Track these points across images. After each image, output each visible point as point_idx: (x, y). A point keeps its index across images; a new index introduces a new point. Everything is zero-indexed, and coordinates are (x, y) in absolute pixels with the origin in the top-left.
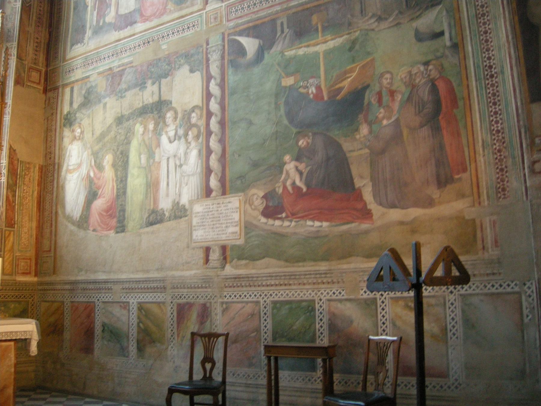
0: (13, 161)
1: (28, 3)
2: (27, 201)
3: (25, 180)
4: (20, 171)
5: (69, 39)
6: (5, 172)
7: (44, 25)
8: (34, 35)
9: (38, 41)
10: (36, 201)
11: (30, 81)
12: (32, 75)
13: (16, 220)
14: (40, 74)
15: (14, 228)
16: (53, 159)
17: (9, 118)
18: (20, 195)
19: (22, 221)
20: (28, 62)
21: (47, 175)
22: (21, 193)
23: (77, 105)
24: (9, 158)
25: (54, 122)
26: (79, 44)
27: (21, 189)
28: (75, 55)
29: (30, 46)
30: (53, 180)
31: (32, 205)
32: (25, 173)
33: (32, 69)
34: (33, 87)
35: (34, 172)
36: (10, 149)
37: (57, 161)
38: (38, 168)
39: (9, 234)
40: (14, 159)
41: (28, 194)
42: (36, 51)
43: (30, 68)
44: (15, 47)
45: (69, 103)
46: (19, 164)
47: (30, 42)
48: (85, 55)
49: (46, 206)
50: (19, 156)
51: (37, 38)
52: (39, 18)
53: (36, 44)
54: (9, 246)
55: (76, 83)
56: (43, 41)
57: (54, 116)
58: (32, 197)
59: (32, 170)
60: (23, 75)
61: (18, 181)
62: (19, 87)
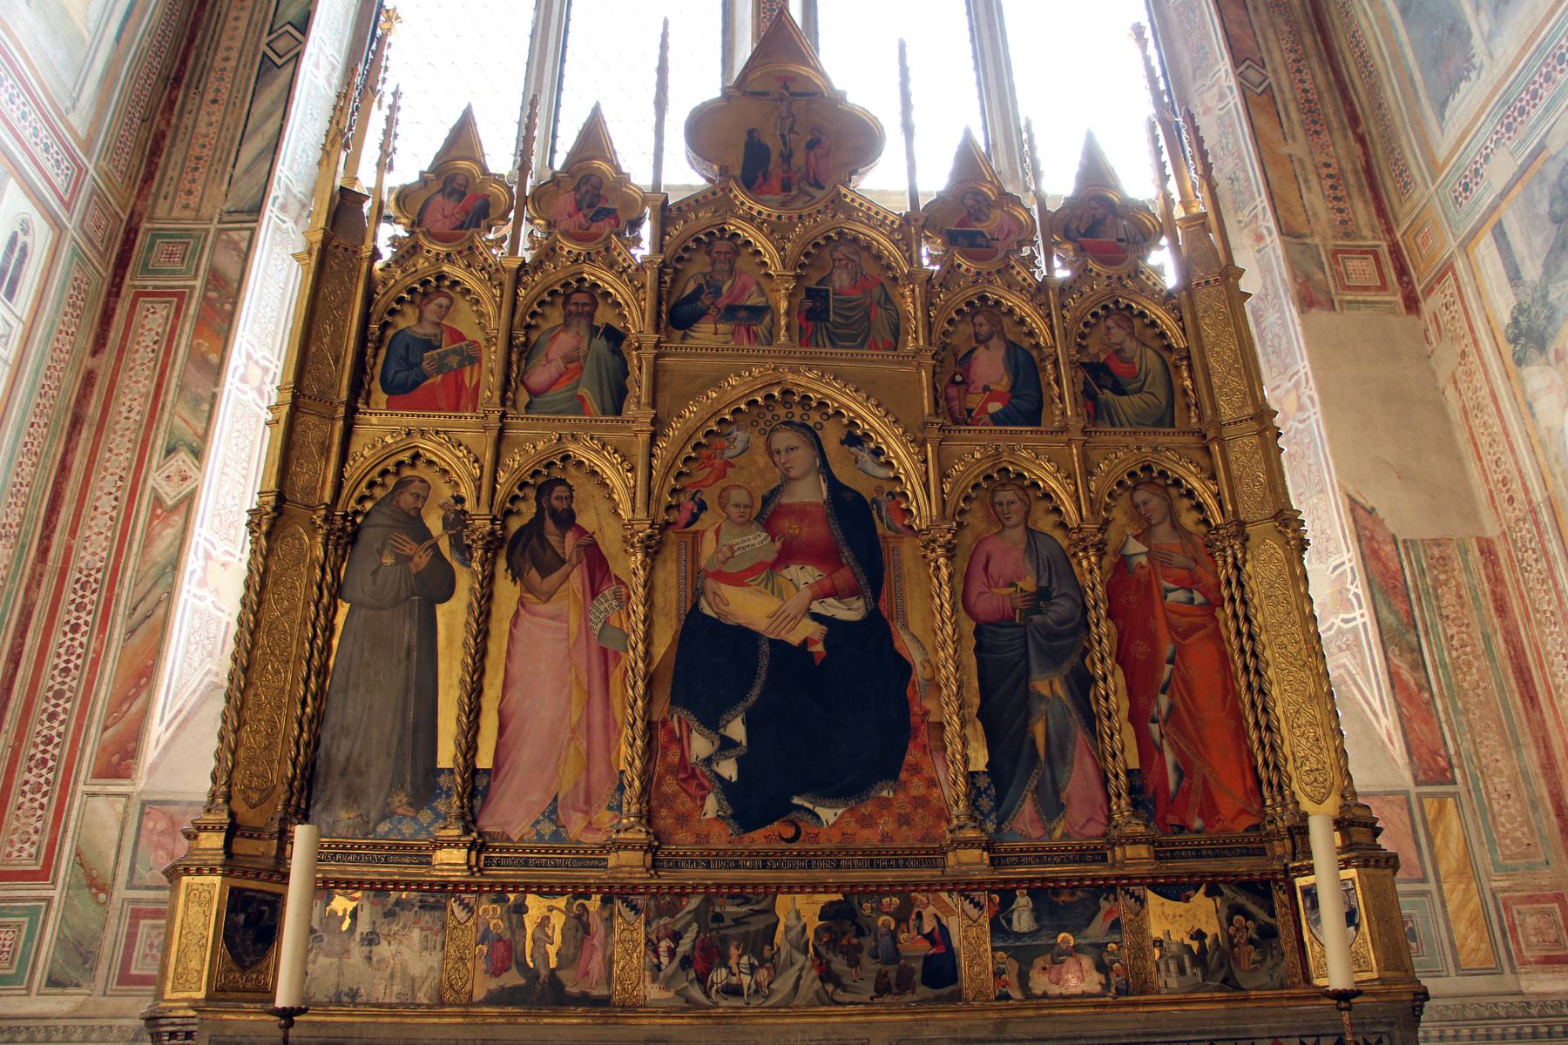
0: (1376, 546)
1: (1261, 84)
2: (1476, 677)
3: (1444, 603)
4: (1413, 574)
5: (1424, 100)
6: (1360, 591)
7: (1335, 125)
8: (1313, 159)
9: (1331, 171)
10: (1510, 671)
11: (1349, 288)
12: (1350, 270)
13: (1452, 751)
14: (1377, 259)
15: (1454, 782)
16: (1520, 496)
17: (1319, 415)
18: (1442, 659)
19: (1477, 752)
20: (1323, 236)
21: (1520, 561)
22: (1441, 650)
23: (1539, 262)
24: (1359, 540)
25: (1479, 377)
26: (1464, 86)
27: (1437, 635)
28: (1466, 124)
29: (1309, 189)
30: (1551, 570)
31: (1502, 691)
32: (1436, 579)
33: (1343, 252)
34: (1365, 302)
35: (1467, 568)
36: (1352, 510)
37: (1538, 495)
38: (1477, 553)
39: (1441, 809)
40: (1379, 537)
41: (1468, 649)
42: (1337, 199)
43: (1335, 253)
44: (1264, 208)
45: (1504, 279)
46: (1402, 551)
47: (1306, 181)
48: (1497, 97)
49: (1554, 675)
50: (1391, 526)
51: (1327, 165)
52: (1310, 111)
53: (1330, 182)
54: (1450, 860)
55: (1504, 205)
56: (1347, 167)
57: (1473, 358)
58: (1493, 660)
59: (1457, 564)
60: (1319, 276)
61: (1417, 612)
62: (1319, 316)
